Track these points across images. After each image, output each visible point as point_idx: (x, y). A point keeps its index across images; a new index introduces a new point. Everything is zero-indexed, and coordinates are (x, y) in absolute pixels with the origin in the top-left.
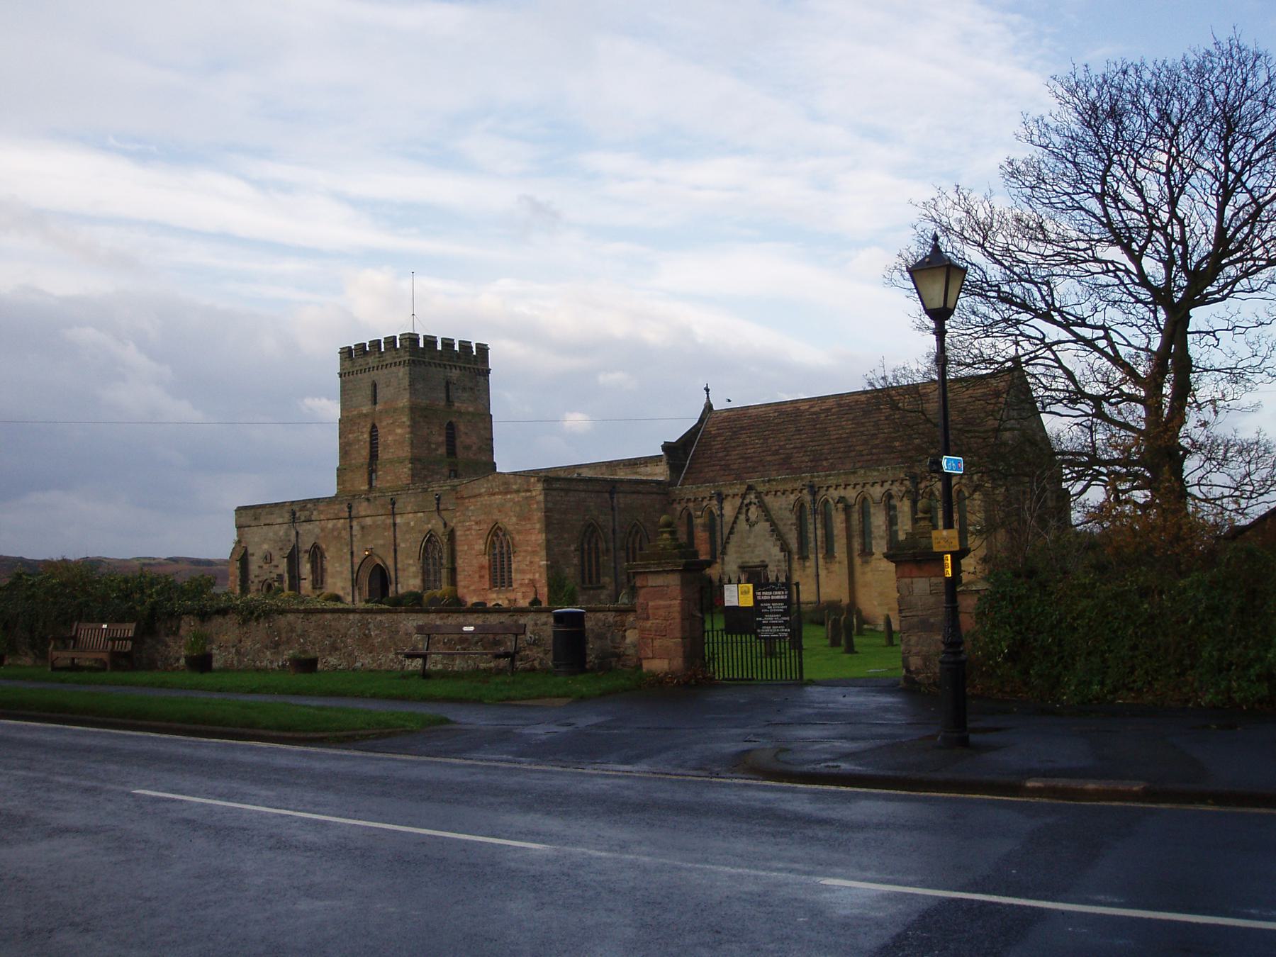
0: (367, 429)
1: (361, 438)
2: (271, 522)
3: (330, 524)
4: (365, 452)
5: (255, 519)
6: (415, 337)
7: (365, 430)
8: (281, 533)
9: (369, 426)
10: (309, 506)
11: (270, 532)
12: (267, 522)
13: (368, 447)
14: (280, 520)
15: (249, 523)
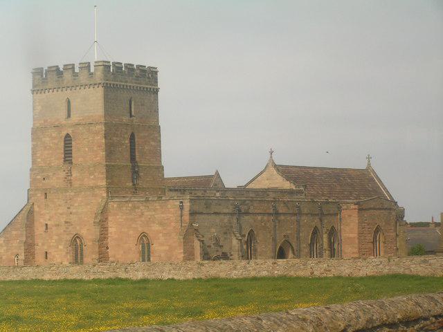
0: (128, 136)
1: (123, 142)
2: (218, 212)
3: (259, 218)
4: (127, 155)
5: (207, 207)
6: (107, 64)
7: (126, 136)
8: (226, 221)
9: (129, 134)
10: (247, 202)
11: (217, 219)
12: (216, 211)
13: (129, 150)
14: (226, 211)
15: (201, 211)
